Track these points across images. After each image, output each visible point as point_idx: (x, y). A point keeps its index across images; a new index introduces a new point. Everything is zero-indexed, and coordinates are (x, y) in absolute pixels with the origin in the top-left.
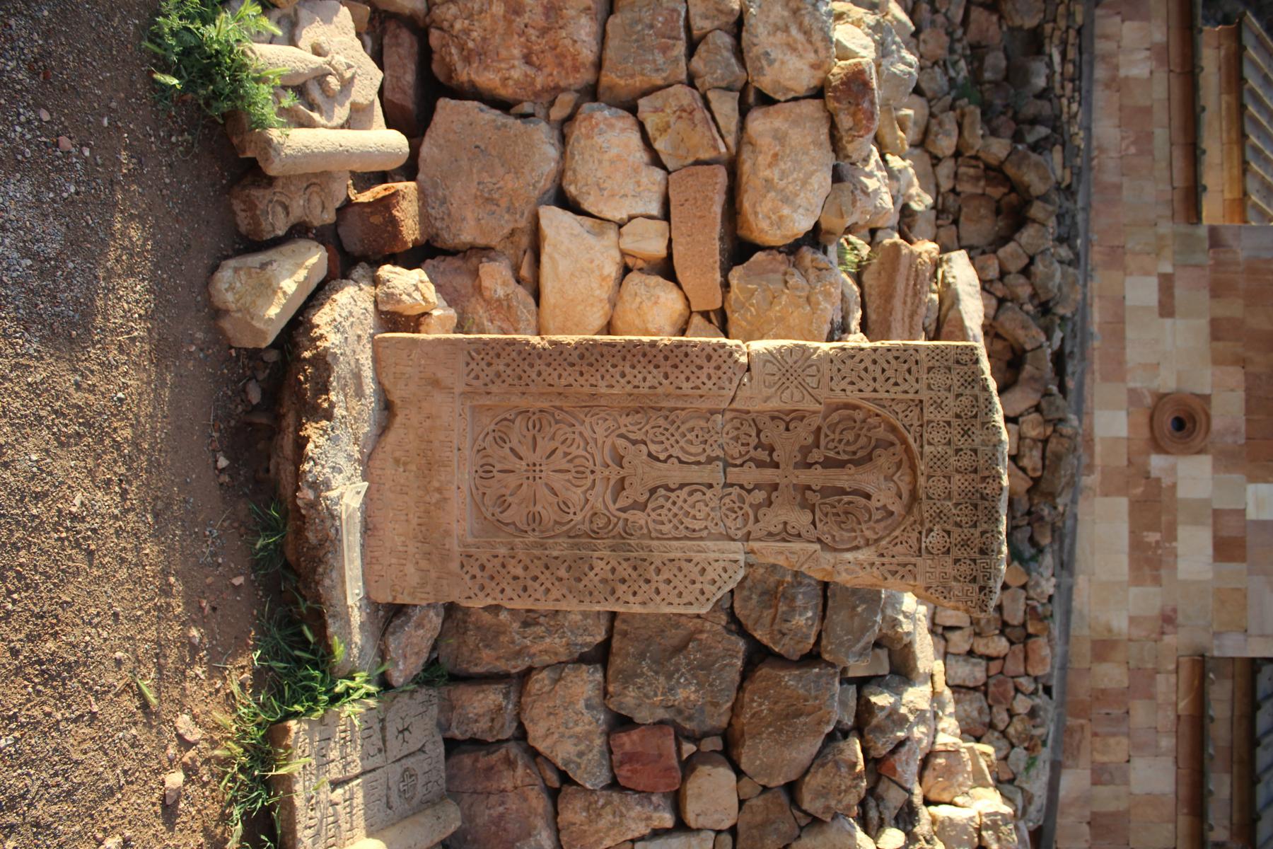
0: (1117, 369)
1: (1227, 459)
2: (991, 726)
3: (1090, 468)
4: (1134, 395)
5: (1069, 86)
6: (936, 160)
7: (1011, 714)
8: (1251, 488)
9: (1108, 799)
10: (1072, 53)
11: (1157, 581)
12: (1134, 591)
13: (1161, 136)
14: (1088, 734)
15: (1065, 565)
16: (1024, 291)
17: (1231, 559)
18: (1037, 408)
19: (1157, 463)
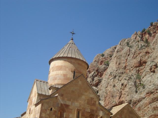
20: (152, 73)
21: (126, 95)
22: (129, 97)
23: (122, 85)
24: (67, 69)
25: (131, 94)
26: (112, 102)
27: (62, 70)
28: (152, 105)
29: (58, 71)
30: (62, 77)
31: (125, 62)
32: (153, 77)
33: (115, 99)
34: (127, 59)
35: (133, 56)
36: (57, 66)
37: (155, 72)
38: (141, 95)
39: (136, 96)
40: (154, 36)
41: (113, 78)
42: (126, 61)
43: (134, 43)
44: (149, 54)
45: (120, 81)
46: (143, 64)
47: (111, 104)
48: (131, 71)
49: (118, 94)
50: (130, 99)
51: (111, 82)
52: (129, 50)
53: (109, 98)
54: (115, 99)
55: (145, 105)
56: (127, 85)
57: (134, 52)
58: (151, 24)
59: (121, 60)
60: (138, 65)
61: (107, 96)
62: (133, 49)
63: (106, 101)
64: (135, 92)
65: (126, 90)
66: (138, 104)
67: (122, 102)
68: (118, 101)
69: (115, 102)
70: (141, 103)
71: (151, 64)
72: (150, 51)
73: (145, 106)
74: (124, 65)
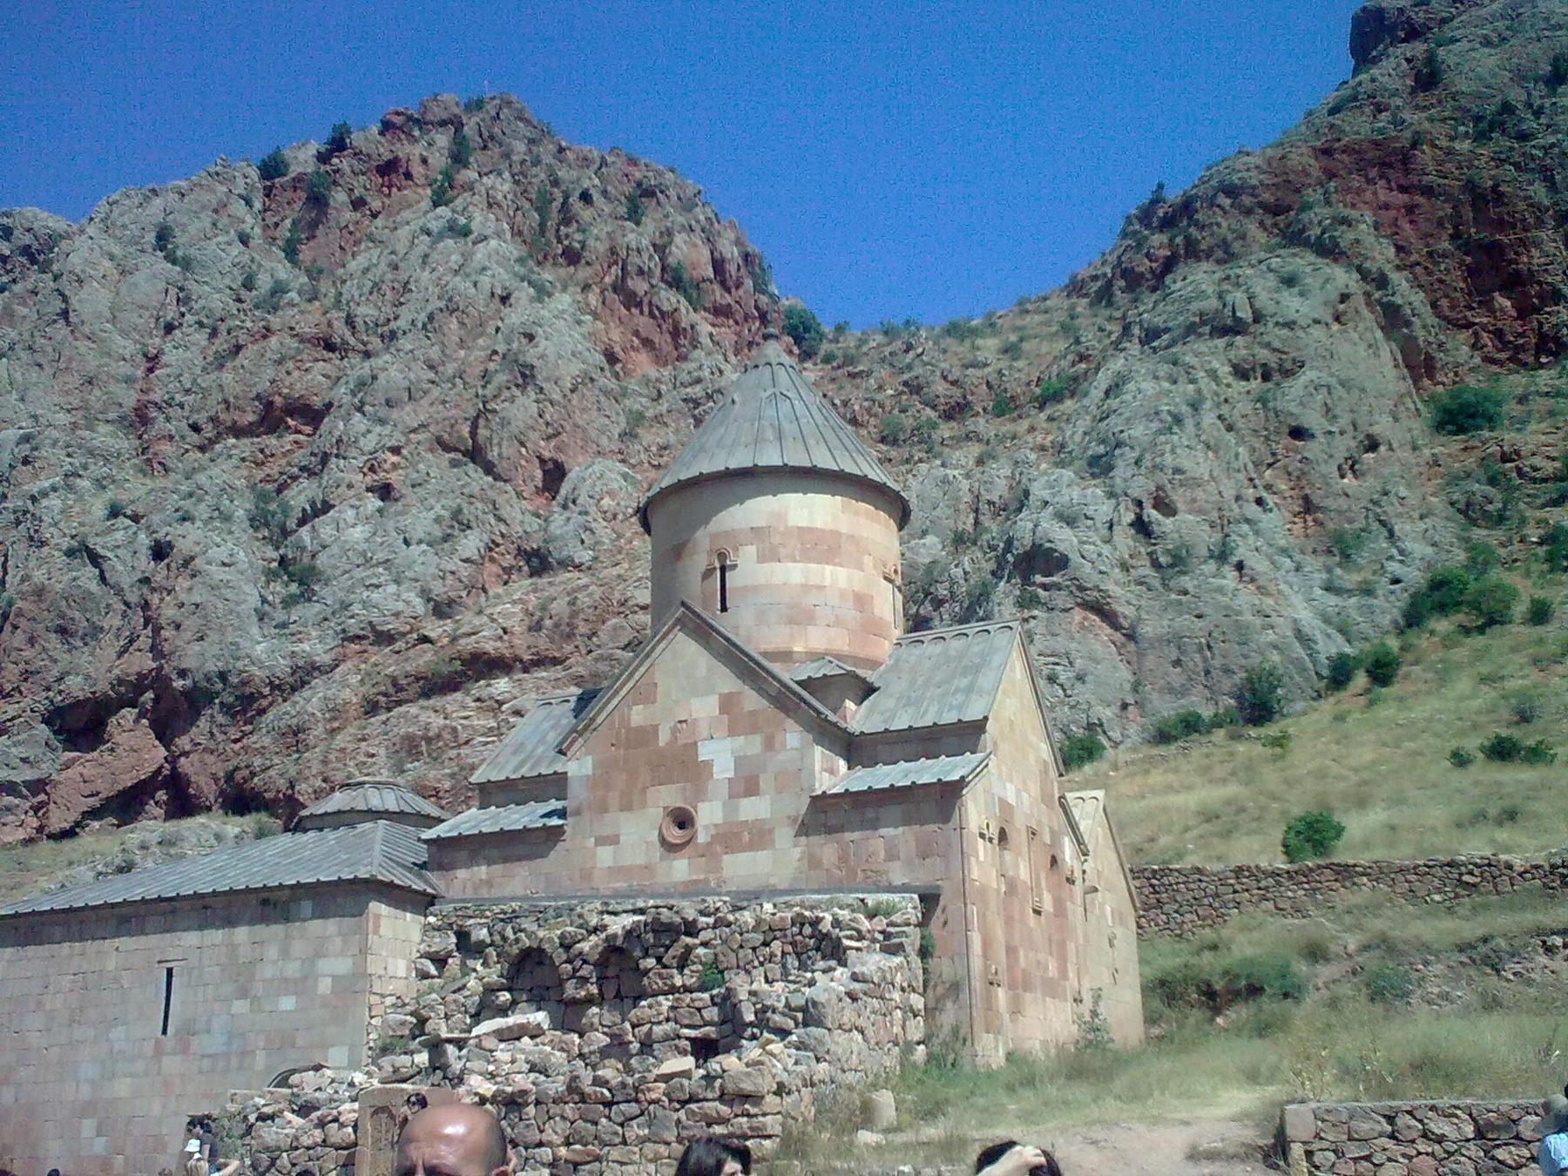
0: (648, 868)
1: (700, 794)
3: (706, 881)
5: (488, 913)
10: (470, 912)
11: (771, 831)
15: (756, 896)
17: (758, 784)
19: (702, 838)
20: (373, 502)
21: (188, 635)
22: (211, 647)
23: (160, 552)
25: (222, 629)
26: (55, 673)
28: (392, 720)
29: (814, 566)
30: (851, 614)
31: (140, 373)
32: (390, 525)
33: (85, 657)
35: (204, 343)
37: (395, 494)
38: (306, 647)
39: (259, 648)
40: (352, 229)
41: (54, 489)
42: (151, 370)
43: (212, 245)
44: (331, 355)
45: (136, 518)
47: (48, 689)
48: (187, 451)
49: (117, 622)
50: (212, 666)
52: (181, 289)
53: (32, 641)
54: (85, 657)
55: (335, 719)
56: (199, 563)
57: (218, 316)
59: (109, 355)
60: (251, 418)
62: (206, 288)
64: (255, 619)
65: (183, 597)
66: (271, 704)
69: (87, 677)
70: (312, 701)
71: (369, 431)
72: (341, 331)
73: (336, 724)
74: (130, 398)
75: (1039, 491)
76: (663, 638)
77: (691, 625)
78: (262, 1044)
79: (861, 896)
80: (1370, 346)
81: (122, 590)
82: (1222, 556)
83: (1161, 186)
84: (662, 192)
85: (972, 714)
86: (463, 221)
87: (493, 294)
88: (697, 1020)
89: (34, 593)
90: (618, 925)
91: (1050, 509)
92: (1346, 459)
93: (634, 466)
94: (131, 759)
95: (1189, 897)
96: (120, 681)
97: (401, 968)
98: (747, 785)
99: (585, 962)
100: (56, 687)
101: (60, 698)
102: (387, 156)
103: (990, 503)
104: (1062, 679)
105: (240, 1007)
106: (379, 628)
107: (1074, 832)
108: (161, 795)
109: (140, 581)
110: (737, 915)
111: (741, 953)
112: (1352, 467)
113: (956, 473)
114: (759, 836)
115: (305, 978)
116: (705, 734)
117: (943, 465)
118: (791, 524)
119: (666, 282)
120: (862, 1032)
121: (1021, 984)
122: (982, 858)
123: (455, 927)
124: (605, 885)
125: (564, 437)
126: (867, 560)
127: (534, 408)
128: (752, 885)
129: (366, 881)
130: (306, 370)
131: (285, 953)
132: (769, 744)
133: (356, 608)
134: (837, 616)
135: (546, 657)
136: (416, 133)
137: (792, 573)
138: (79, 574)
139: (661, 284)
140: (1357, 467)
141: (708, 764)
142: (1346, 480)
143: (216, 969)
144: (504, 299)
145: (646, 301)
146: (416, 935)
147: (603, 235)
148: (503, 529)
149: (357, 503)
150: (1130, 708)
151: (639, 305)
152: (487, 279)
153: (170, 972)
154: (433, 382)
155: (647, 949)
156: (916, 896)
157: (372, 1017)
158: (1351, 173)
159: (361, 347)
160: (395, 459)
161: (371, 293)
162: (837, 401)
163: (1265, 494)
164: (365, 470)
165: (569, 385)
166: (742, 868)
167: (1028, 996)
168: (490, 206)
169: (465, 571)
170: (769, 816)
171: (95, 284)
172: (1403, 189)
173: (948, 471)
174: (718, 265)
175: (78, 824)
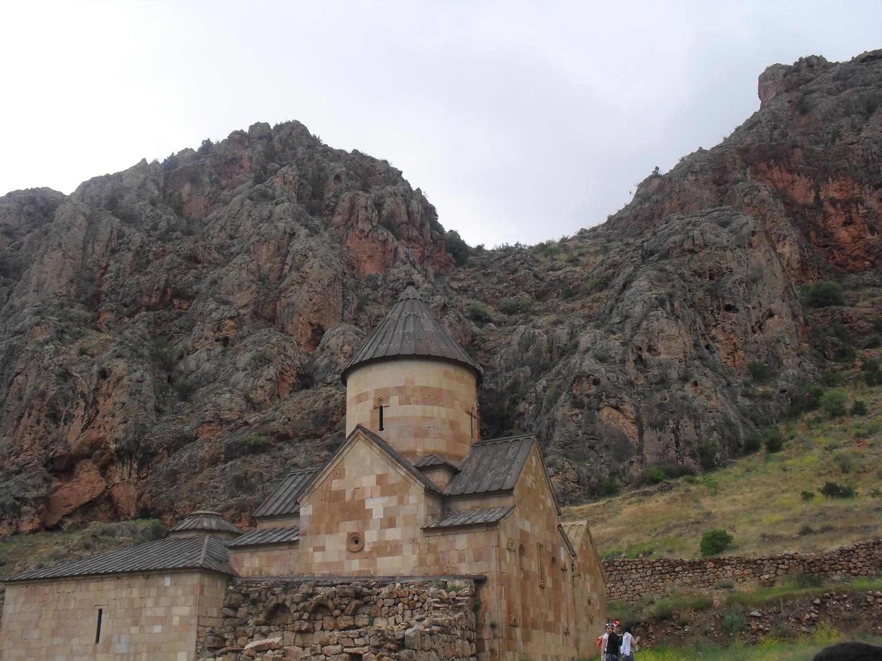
0: (340, 564)
1: (366, 525)
2: (421, 607)
4: (348, 558)
6: (270, 631)
7: (418, 601)
8: (374, 517)
9: (469, 556)
11: (401, 546)
12: (404, 553)
13: (276, 553)
14: (448, 565)
15: (393, 579)
16: (302, 604)
18: (332, 599)
19: (367, 549)
20: (219, 348)
21: (118, 420)
23: (104, 374)
24: (457, 402)
27: (442, 406)
28: (228, 469)
29: (428, 407)
32: (228, 360)
34: (106, 268)
36: (422, 388)
40: (211, 195)
42: (103, 274)
44: (199, 266)
46: (171, 301)
49: (81, 413)
51: (47, 357)
53: (38, 422)
55: (196, 467)
57: (138, 245)
58: (203, 143)
61: (26, 415)
63: (18, 433)
65: (116, 399)
67: (96, 443)
68: (78, 438)
71: (217, 308)
73: (197, 470)
75: (585, 340)
76: (348, 445)
77: (362, 438)
78: (145, 649)
79: (445, 580)
80: (769, 260)
81: (84, 395)
82: (685, 379)
83: (657, 168)
84: (380, 174)
85: (507, 486)
86: (270, 191)
87: (286, 232)
88: (352, 644)
89: (39, 396)
90: (322, 592)
91: (590, 353)
92: (756, 323)
93: (361, 327)
94: (89, 487)
95: (637, 576)
96: (83, 443)
97: (214, 612)
98: (390, 522)
99: (305, 611)
100: (51, 447)
101: (52, 453)
102: (230, 157)
103: (559, 347)
104: (597, 447)
105: (134, 630)
106: (221, 417)
107: (567, 544)
108: (103, 506)
109: (94, 390)
110: (383, 589)
111: (383, 609)
112: (760, 327)
113: (540, 331)
114: (394, 549)
115: (166, 617)
116: (369, 494)
117: (534, 327)
118: (416, 385)
119: (382, 225)
120: (436, 651)
121: (529, 626)
122: (508, 561)
123: (243, 592)
124: (319, 572)
125: (323, 312)
126: (457, 402)
127: (306, 296)
128: (391, 573)
129: (197, 568)
130: (185, 274)
131: (156, 603)
132: (401, 501)
133: (209, 406)
134: (440, 433)
135: (312, 434)
136: (247, 144)
137: (416, 410)
138: (63, 386)
139: (380, 226)
140: (763, 327)
141: (370, 511)
142: (757, 335)
143: (123, 610)
144: (292, 235)
145: (370, 235)
146: (222, 596)
147: (347, 199)
148: (289, 362)
149: (211, 348)
150: (635, 464)
151: (367, 236)
152: (283, 225)
153: (100, 611)
154: (253, 281)
155: (336, 606)
156: (472, 581)
157: (199, 637)
158: (760, 163)
159: (213, 261)
160: (231, 323)
161: (220, 231)
162: (476, 290)
163: (711, 343)
164: (215, 330)
165: (326, 283)
166: (386, 566)
167: (535, 632)
168: (285, 184)
169: (269, 386)
170: (400, 538)
171: (76, 229)
172: (790, 171)
173: (537, 331)
174: (409, 214)
175: (61, 522)
